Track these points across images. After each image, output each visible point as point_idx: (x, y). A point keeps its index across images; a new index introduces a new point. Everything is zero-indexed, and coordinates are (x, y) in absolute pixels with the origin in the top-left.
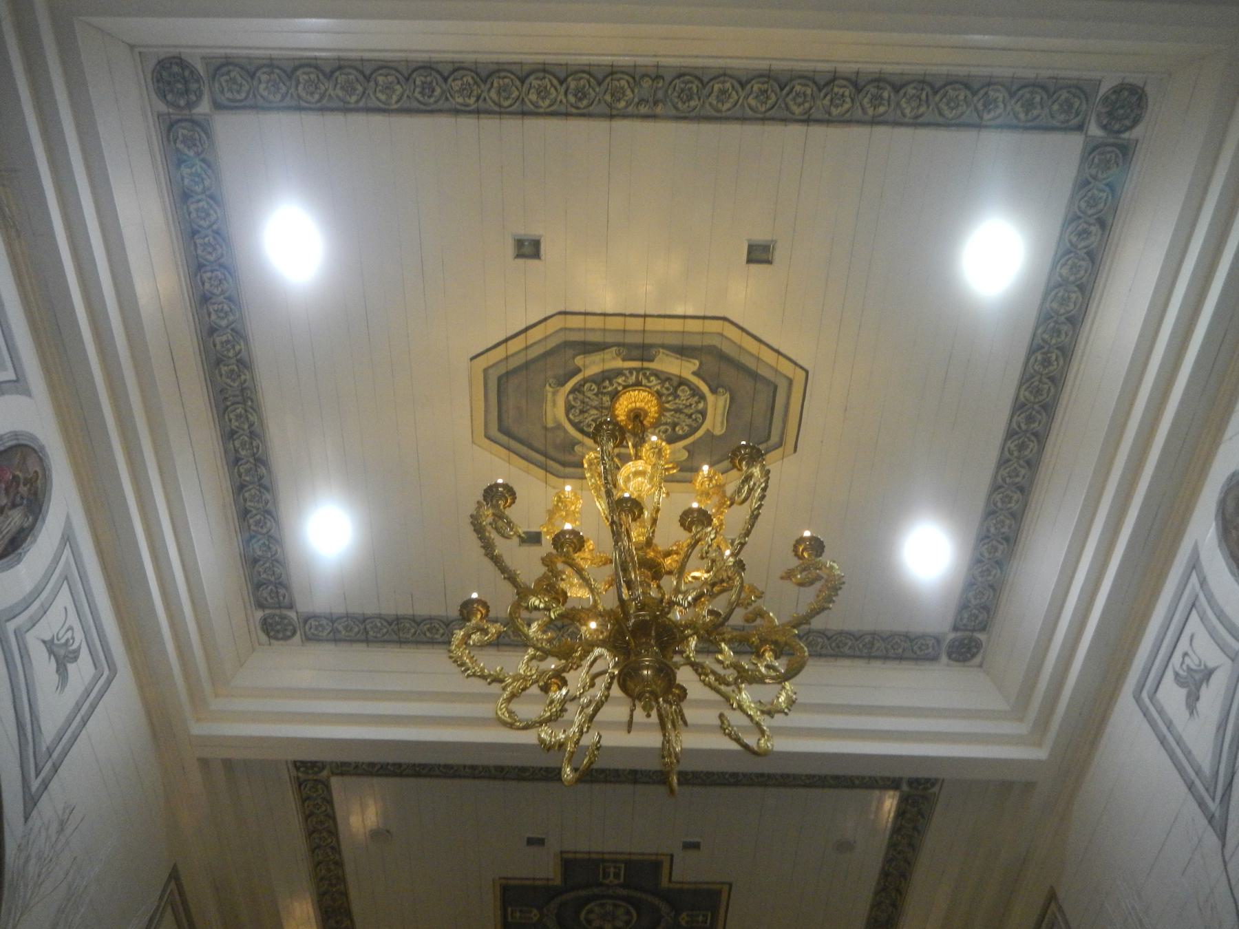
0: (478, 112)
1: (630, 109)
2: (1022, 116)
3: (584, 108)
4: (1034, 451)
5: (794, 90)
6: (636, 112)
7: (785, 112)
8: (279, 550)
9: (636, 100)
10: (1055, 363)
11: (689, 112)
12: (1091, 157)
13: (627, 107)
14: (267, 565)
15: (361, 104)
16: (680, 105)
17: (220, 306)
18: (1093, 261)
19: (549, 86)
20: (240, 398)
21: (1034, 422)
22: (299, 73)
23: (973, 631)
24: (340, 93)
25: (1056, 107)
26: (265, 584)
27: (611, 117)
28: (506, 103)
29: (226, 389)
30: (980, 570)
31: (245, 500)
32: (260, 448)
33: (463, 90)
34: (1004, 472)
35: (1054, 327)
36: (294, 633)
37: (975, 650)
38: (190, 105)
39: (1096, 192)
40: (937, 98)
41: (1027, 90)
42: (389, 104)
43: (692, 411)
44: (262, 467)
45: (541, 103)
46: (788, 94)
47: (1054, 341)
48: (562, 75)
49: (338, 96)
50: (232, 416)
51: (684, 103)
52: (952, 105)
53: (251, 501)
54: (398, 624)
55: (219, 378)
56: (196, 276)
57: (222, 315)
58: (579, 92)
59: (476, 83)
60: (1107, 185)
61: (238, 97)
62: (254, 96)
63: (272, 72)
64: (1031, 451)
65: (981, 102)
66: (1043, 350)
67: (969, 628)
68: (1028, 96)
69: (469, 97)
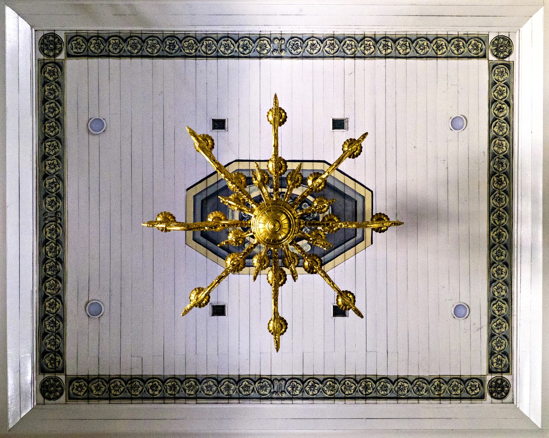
0: (196, 57)
1: (269, 54)
2: (456, 52)
3: (247, 54)
4: (507, 238)
5: (346, 43)
6: (272, 55)
7: (343, 53)
8: (61, 326)
9: (272, 50)
10: (505, 182)
11: (298, 54)
12: (493, 71)
13: (267, 53)
14: (52, 337)
15: (139, 54)
16: (293, 51)
17: (52, 162)
18: (509, 123)
19: (230, 44)
20: (53, 219)
21: (503, 219)
22: (110, 39)
23: (502, 372)
24: (129, 48)
25: (470, 47)
26: (48, 352)
27: (260, 58)
28: (210, 52)
29: (47, 212)
30: (495, 324)
31: (46, 289)
32: (61, 251)
33: (190, 46)
34: (494, 253)
35: (499, 161)
36: (61, 394)
37: (507, 389)
38: (55, 55)
39: (501, 87)
40: (414, 45)
41: (456, 40)
42: (152, 54)
43: (311, 218)
44: (60, 264)
45: (226, 52)
46: (344, 45)
47: (501, 169)
48: (236, 39)
49: (128, 50)
50: (47, 230)
51: (295, 50)
52: (421, 48)
53: (49, 289)
54: (131, 383)
55: (44, 205)
56: (42, 144)
57: (53, 166)
58: (245, 46)
59: (195, 43)
60: (504, 83)
61: (80, 51)
62: (88, 50)
63: (98, 39)
64: (506, 237)
65: (435, 46)
66: (497, 175)
67: (499, 370)
68: (456, 42)
69: (192, 50)
